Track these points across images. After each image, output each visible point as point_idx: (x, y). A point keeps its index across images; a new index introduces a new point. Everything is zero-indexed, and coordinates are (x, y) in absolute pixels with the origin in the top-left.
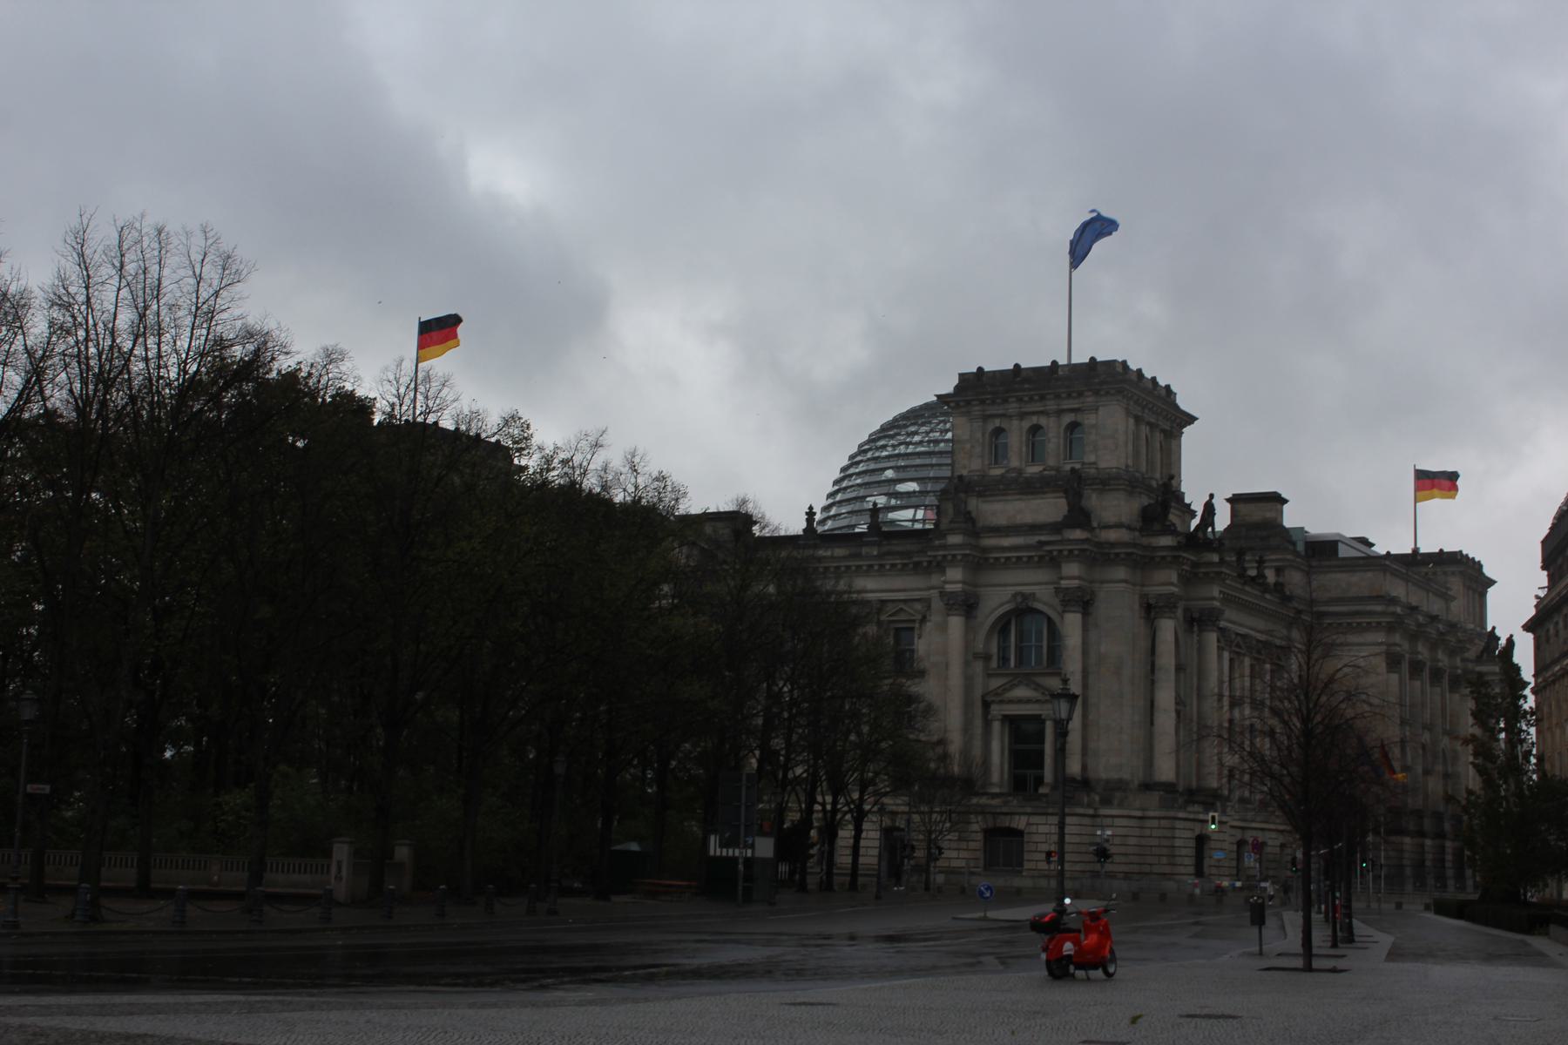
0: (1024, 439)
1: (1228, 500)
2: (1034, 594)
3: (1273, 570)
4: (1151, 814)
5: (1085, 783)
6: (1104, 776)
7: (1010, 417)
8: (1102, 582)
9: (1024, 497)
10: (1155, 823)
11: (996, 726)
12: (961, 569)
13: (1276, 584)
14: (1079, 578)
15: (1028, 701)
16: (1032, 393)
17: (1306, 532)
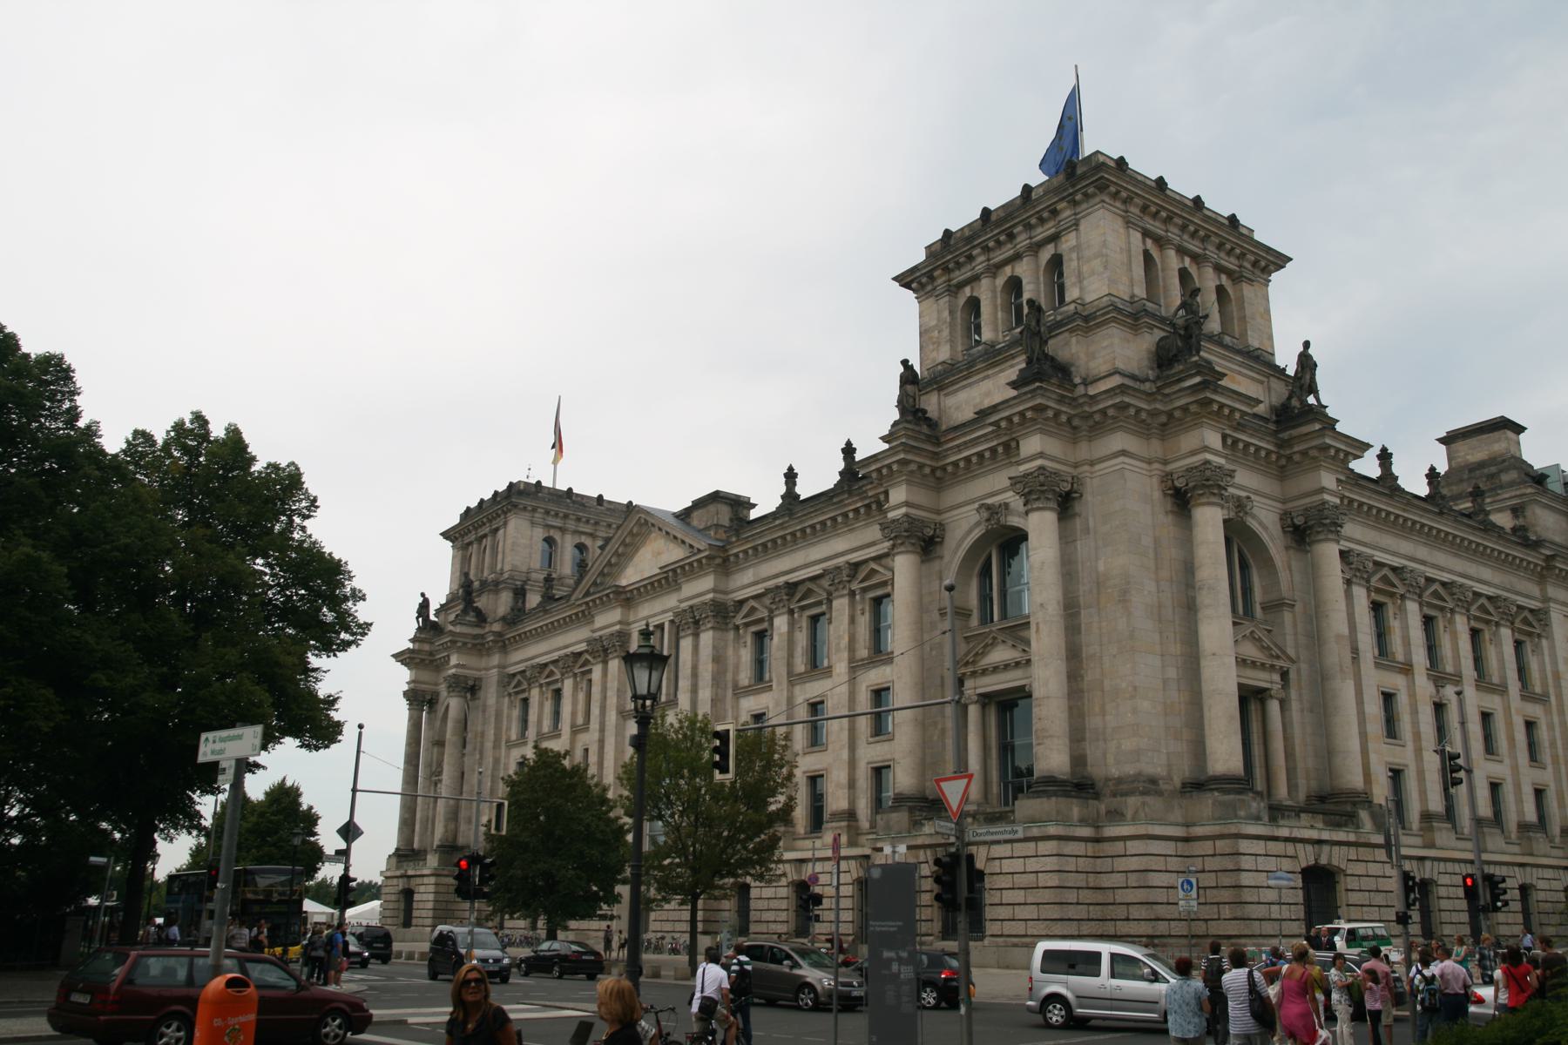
0: (999, 301)
1: (1442, 441)
2: (1006, 505)
3: (1509, 512)
4: (1198, 831)
5: (1080, 786)
6: (1115, 772)
7: (975, 278)
8: (1092, 464)
9: (990, 372)
10: (1207, 847)
11: (973, 711)
12: (904, 486)
13: (1514, 530)
14: (1041, 455)
15: (1007, 667)
16: (995, 232)
17: (1563, 471)
